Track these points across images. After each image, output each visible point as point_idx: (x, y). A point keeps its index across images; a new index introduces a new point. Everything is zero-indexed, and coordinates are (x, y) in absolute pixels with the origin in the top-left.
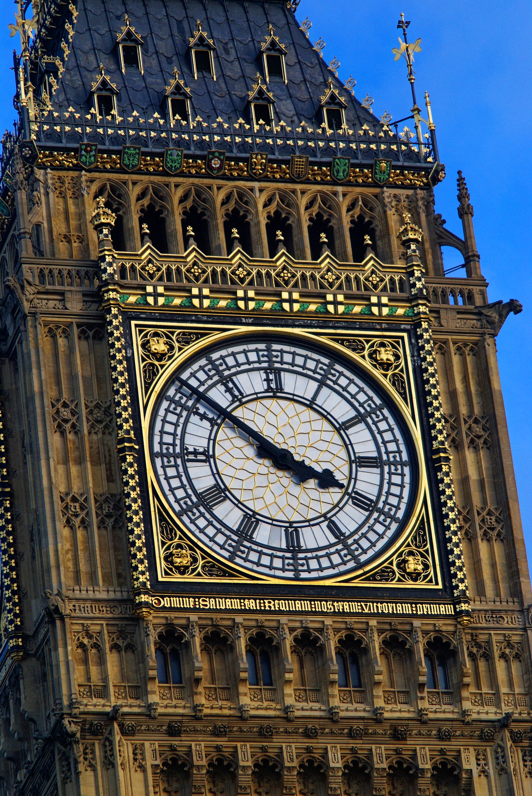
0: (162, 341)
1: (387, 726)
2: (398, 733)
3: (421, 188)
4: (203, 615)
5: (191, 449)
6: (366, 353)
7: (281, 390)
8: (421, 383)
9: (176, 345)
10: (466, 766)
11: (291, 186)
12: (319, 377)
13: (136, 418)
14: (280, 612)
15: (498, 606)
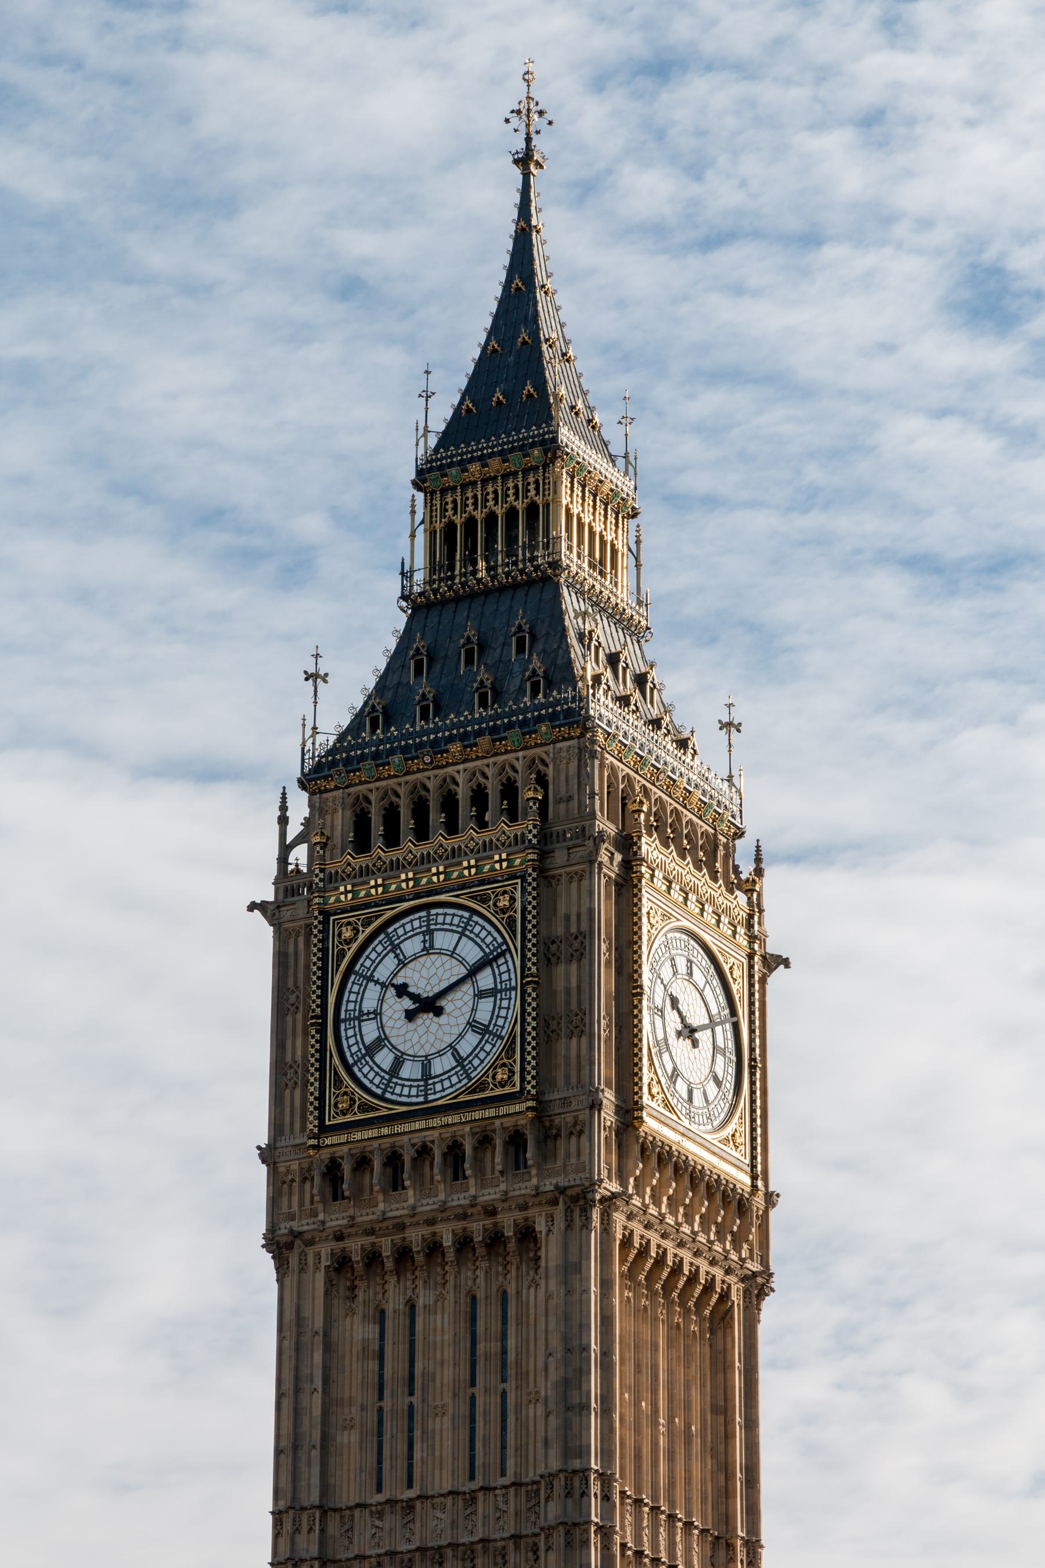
0: (349, 927)
1: (479, 1208)
2: (491, 1212)
3: (578, 738)
4: (351, 1146)
5: (365, 1011)
6: (491, 903)
7: (432, 947)
8: (524, 918)
9: (361, 929)
10: (537, 1229)
11: (485, 761)
12: (460, 929)
13: (324, 997)
14: (405, 1133)
15: (570, 1093)
